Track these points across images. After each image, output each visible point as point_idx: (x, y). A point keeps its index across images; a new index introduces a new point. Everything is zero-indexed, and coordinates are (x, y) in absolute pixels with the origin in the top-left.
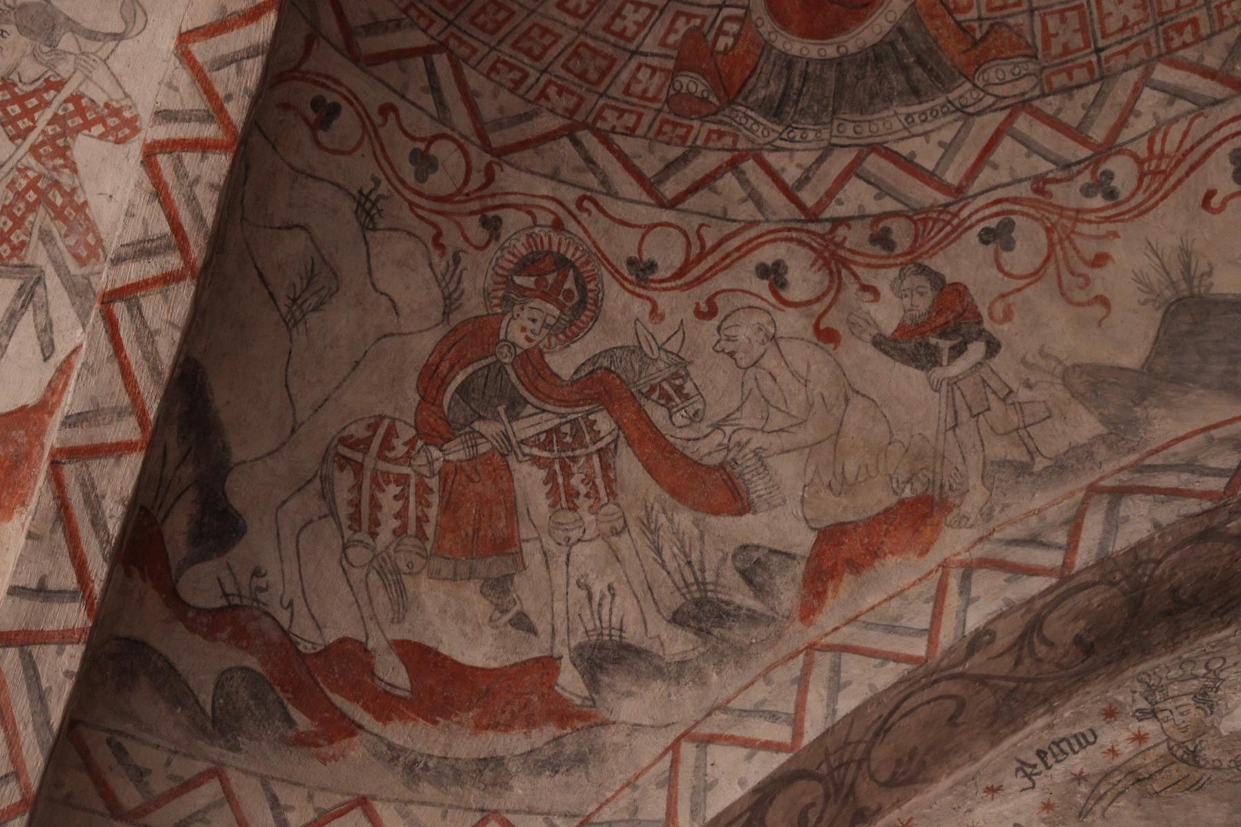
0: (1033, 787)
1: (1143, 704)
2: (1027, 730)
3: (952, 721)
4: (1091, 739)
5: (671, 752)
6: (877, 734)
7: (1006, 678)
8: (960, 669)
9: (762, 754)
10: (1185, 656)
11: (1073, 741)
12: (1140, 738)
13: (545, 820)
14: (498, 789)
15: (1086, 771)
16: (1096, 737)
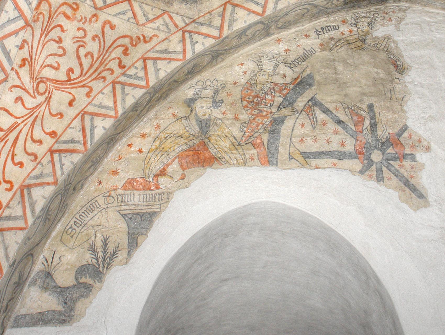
0: (319, 38)
1: (354, 22)
2: (320, 20)
3: (303, 15)
4: (337, 28)
5: (223, 6)
6: (284, 15)
7: (322, 7)
8: (313, 3)
9: (252, 15)
10: (368, 10)
11: (332, 27)
12: (351, 31)
13: (182, 17)
14: (169, 5)
15: (334, 37)
16: (339, 28)
